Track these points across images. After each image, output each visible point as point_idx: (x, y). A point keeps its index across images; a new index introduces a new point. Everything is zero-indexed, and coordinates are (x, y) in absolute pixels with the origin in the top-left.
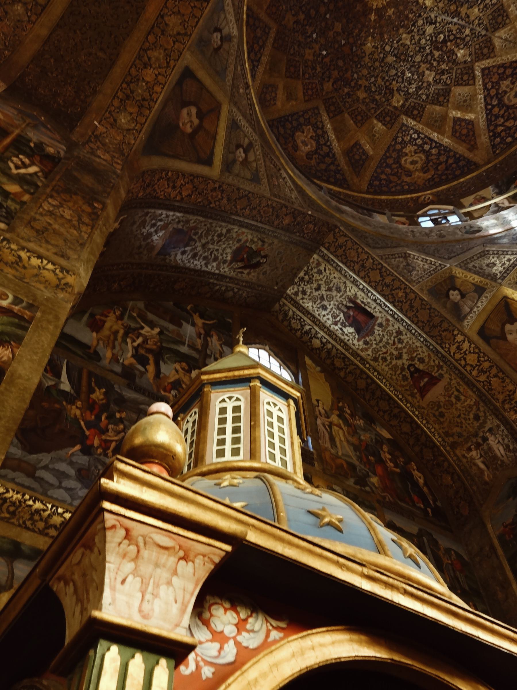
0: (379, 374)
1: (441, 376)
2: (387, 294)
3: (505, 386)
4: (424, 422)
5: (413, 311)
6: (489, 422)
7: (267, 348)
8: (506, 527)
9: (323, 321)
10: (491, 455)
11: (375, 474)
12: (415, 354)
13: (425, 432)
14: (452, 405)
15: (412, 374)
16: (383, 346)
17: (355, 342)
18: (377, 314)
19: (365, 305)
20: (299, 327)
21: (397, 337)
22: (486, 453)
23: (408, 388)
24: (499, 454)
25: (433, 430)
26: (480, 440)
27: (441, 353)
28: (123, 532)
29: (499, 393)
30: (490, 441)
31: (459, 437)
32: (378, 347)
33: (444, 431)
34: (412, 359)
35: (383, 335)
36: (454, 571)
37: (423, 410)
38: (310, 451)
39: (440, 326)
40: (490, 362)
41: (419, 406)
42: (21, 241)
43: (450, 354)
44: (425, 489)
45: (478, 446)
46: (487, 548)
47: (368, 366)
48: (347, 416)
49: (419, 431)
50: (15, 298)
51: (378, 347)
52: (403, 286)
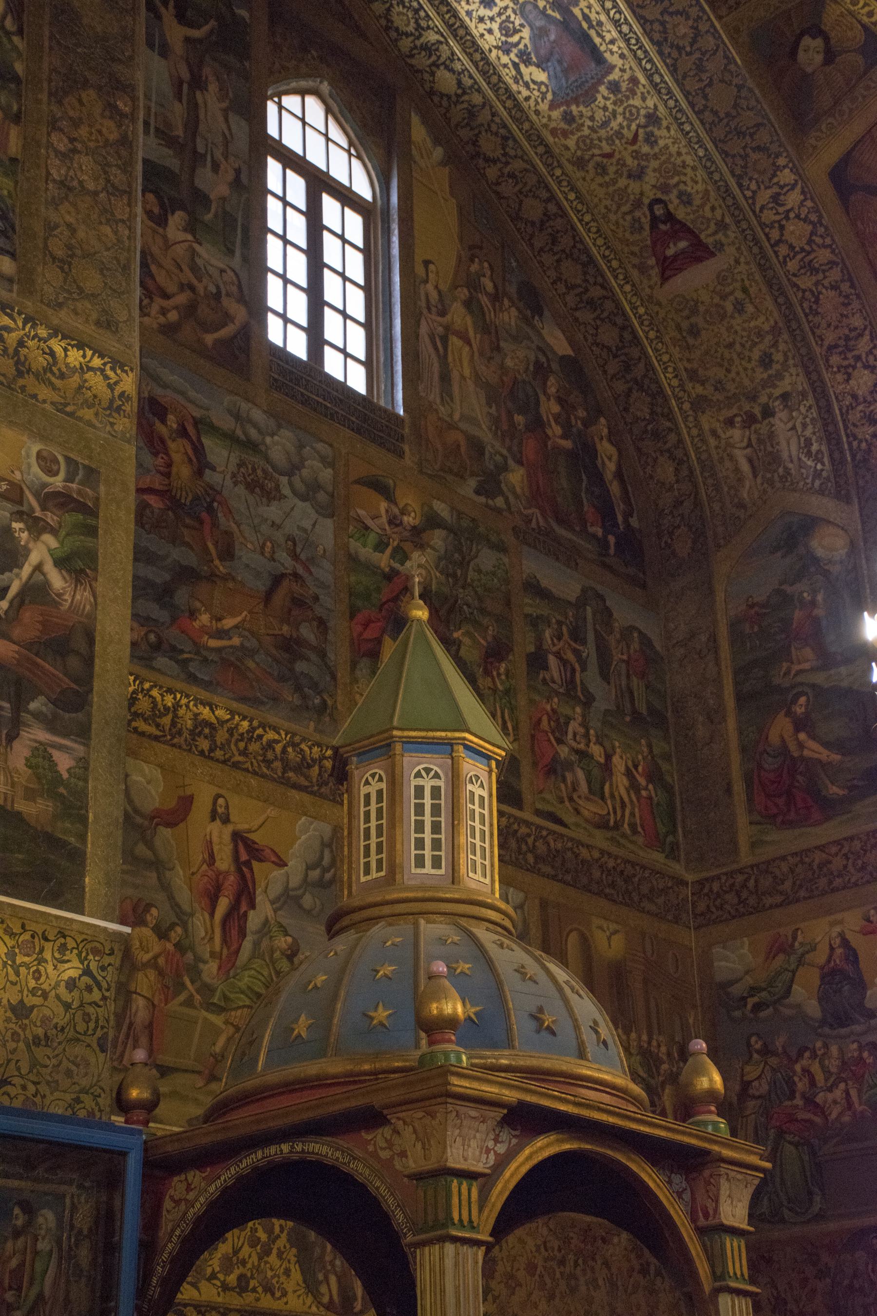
0: (579, 198)
1: (720, 246)
2: (650, 17)
3: (847, 316)
4: (652, 334)
5: (701, 80)
6: (787, 380)
7: (325, 87)
8: (751, 606)
9: (475, 32)
10: (769, 449)
11: (520, 463)
12: (676, 179)
13: (647, 357)
14: (723, 317)
15: (655, 221)
16: (607, 139)
17: (544, 107)
18: (614, 60)
19: (591, 26)
20: (411, 28)
21: (645, 127)
22: (760, 441)
23: (636, 249)
24: (785, 455)
25: (665, 358)
26: (757, 411)
27: (734, 198)
28: (454, 1114)
29: (829, 325)
30: (776, 421)
31: (716, 389)
32: (595, 136)
33: (689, 366)
34: (665, 188)
35: (614, 114)
36: (628, 677)
37: (656, 308)
38: (397, 416)
39: (751, 135)
40: (833, 252)
41: (650, 297)
42: (50, 312)
43: (752, 206)
44: (615, 488)
45: (750, 420)
46: (703, 638)
47: (558, 172)
48: (485, 300)
49: (635, 352)
50: (68, 459)
51: (595, 136)
52: (694, 12)
